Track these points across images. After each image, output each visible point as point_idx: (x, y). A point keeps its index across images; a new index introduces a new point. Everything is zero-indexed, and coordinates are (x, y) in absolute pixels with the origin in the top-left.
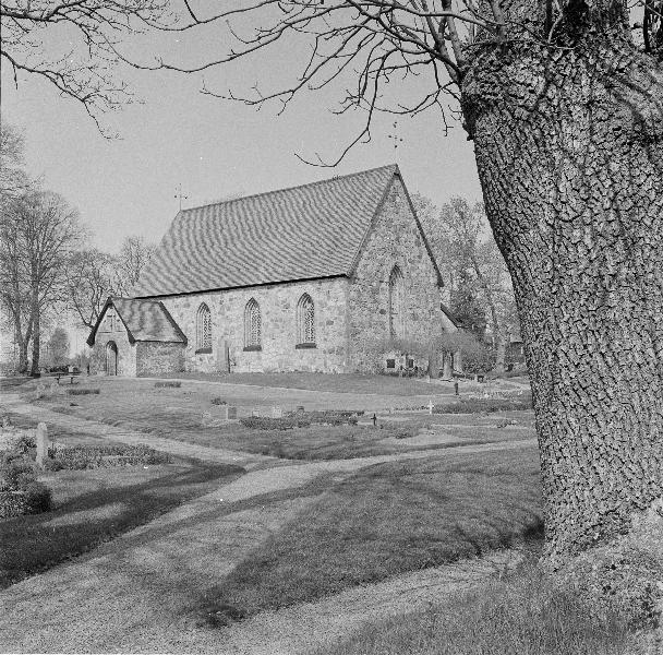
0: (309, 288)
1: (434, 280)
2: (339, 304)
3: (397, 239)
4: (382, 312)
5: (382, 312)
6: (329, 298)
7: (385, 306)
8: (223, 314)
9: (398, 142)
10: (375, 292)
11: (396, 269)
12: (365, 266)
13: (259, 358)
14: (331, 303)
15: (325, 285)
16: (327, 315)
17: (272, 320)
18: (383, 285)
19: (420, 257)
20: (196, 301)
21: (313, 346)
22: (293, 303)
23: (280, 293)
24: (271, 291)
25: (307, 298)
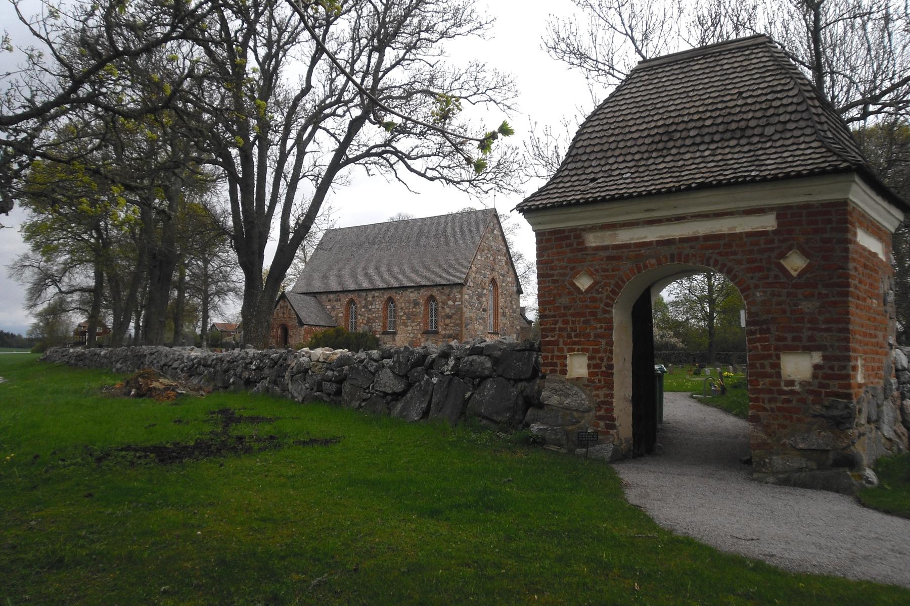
0: (435, 292)
1: (515, 289)
3: (494, 260)
4: (484, 310)
5: (484, 310)
10: (480, 296)
12: (474, 278)
13: (394, 340)
14: (450, 303)
15: (447, 291)
16: (448, 310)
17: (405, 313)
18: (485, 291)
23: (413, 295)
25: (432, 298)
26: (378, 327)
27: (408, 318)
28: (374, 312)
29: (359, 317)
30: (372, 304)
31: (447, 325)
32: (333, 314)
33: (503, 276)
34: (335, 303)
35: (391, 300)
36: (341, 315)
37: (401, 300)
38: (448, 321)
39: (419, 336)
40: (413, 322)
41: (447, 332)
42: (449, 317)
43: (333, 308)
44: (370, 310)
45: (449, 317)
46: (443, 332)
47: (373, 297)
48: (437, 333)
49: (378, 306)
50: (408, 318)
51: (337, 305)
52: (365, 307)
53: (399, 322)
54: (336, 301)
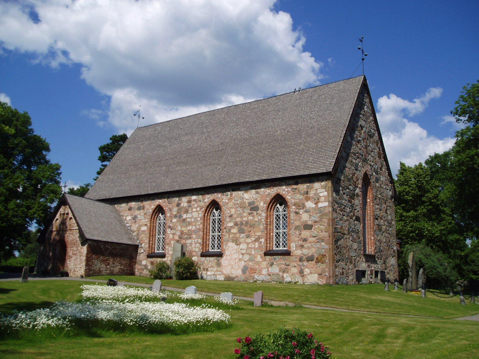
2: (320, 205)
5: (358, 219)
6: (308, 199)
7: (359, 214)
8: (180, 217)
9: (364, 57)
11: (366, 179)
13: (219, 265)
14: (310, 205)
15: (303, 187)
16: (305, 217)
17: (236, 224)
19: (381, 169)
20: (150, 206)
21: (287, 253)
22: (262, 205)
23: (249, 196)
24: (235, 193)
25: (279, 199)
26: (194, 247)
27: (241, 231)
28: (190, 224)
29: (169, 231)
30: (187, 212)
31: (305, 240)
32: (134, 227)
33: (377, 173)
34: (137, 212)
35: (215, 205)
36: (144, 228)
37: (231, 204)
38: (306, 233)
39: (259, 259)
40: (248, 236)
41: (305, 251)
42: (308, 227)
43: (135, 218)
44: (184, 220)
45: (308, 227)
46: (298, 252)
47: (189, 202)
48: (287, 253)
49: (195, 215)
50: (241, 231)
51: (140, 214)
52: (178, 216)
53: (226, 236)
54: (139, 209)
